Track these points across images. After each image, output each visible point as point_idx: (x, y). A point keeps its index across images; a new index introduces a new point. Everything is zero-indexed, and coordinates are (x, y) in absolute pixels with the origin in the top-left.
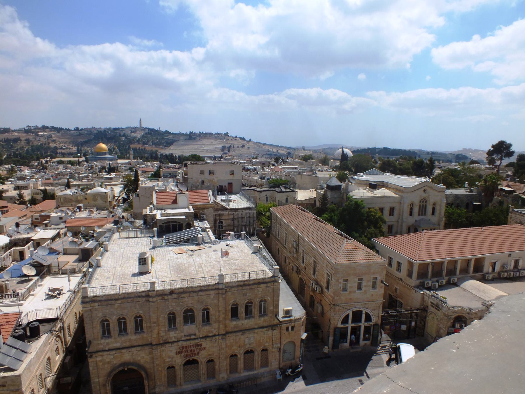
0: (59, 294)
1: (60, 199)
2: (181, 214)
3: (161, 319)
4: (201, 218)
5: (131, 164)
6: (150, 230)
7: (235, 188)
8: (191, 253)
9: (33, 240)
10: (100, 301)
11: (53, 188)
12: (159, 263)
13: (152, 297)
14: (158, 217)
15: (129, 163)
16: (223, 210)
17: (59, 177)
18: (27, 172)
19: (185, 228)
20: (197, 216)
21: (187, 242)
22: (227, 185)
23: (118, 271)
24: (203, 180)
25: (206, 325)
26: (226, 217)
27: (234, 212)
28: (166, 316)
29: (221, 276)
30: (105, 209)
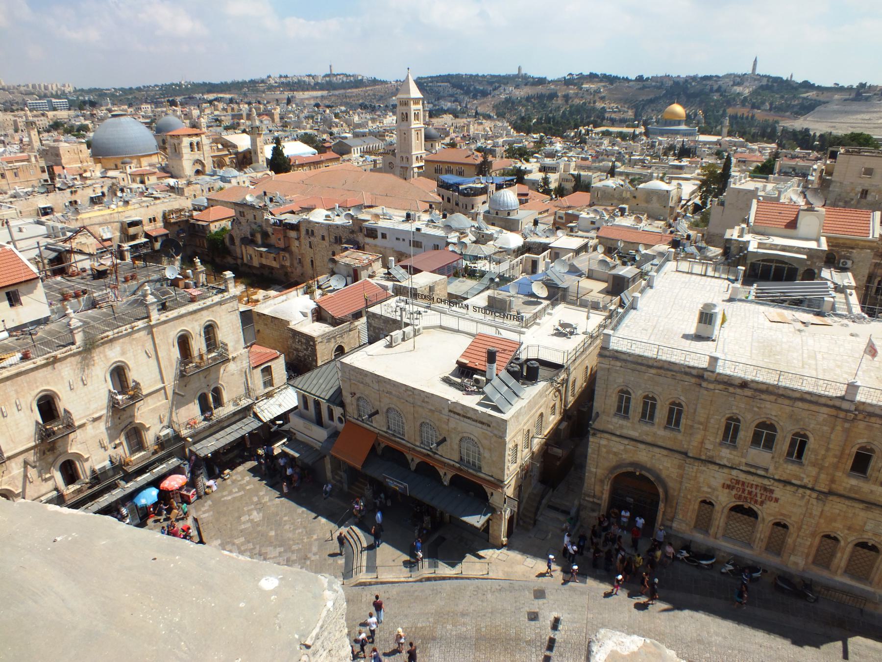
0: (572, 333)
2: (799, 250)
3: (712, 421)
4: (841, 265)
5: (720, 145)
6: (732, 268)
8: (801, 327)
9: (551, 248)
10: (625, 361)
11: (590, 174)
14: (752, 247)
15: (718, 143)
17: (600, 157)
18: (558, 146)
19: (800, 278)
20: (832, 259)
21: (797, 303)
24: (865, 188)
25: (793, 462)
28: (723, 420)
29: (852, 387)
30: (662, 218)
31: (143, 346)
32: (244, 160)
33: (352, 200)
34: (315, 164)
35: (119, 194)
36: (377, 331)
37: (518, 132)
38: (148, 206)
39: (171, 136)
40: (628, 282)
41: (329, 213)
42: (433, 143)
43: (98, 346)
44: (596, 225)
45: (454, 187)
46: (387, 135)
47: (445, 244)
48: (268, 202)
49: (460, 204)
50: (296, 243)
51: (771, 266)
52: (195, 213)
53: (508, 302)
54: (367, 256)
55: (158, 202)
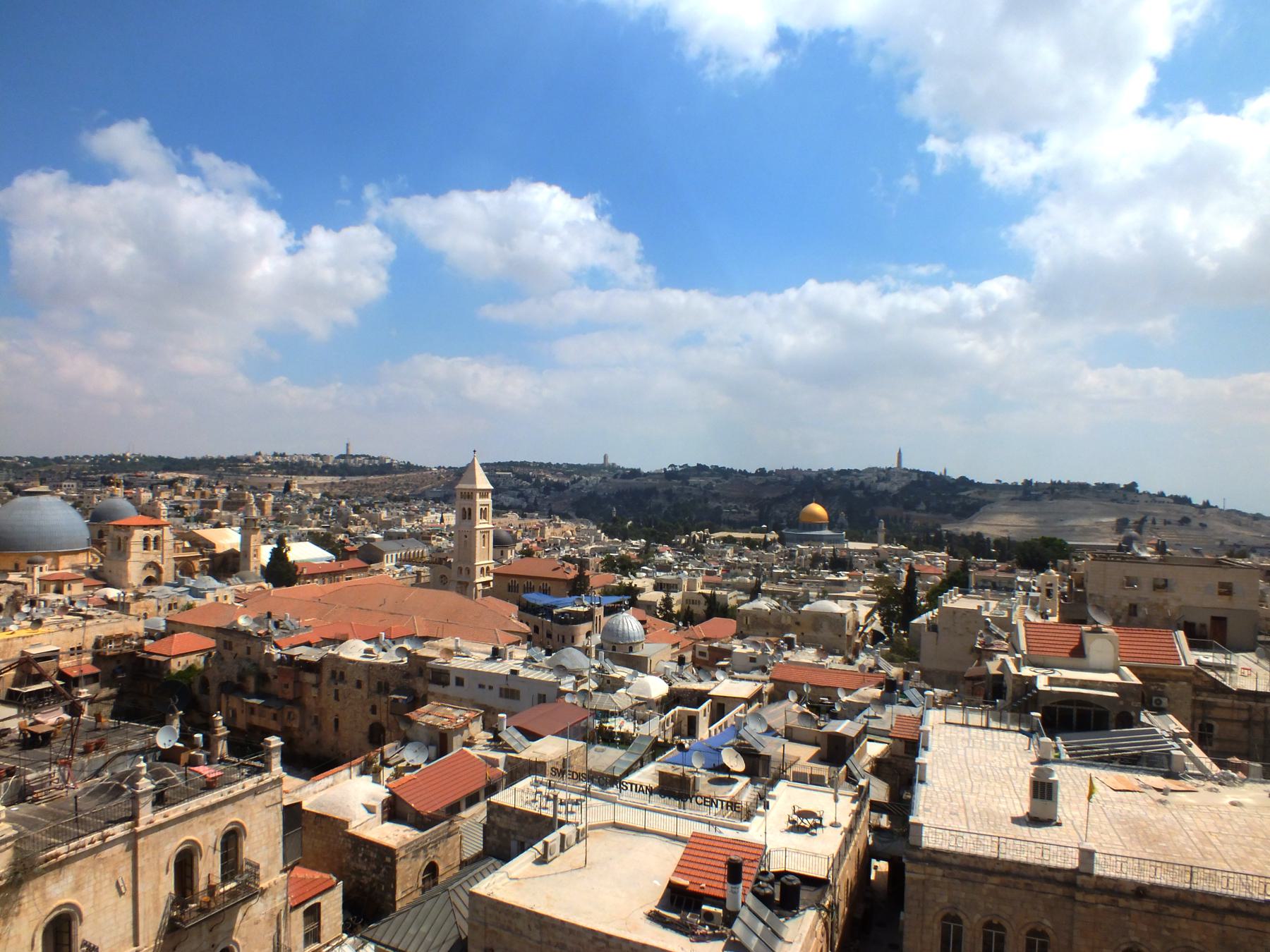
0: (816, 826)
1: (745, 618)
4: (1154, 705)
5: (878, 554)
7: (1233, 630)
8: (1159, 796)
9: (712, 697)
10: (950, 866)
11: (724, 593)
12: (1074, 805)
13: (1082, 889)
15: (873, 551)
16: (1213, 691)
17: (732, 571)
18: (668, 556)
19: (1113, 725)
21: (1131, 762)
22: (1208, 622)
23: (973, 803)
24: (1133, 602)
26: (1225, 714)
27: (1253, 704)
31: (115, 872)
32: (225, 566)
33: (398, 628)
34: (330, 575)
35: (25, 609)
36: (504, 835)
38: (72, 629)
39: (115, 526)
40: (853, 742)
41: (371, 646)
42: (504, 550)
43: (36, 876)
44: (759, 663)
45: (547, 611)
46: (434, 538)
48: (273, 629)
49: (555, 635)
50: (314, 692)
51: (1072, 710)
52: (147, 642)
53: (692, 780)
55: (89, 622)
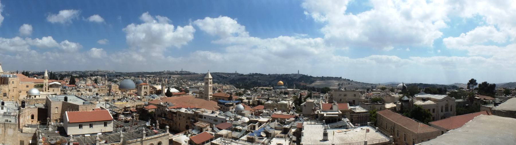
8: (345, 132)
11: (261, 100)
14: (325, 115)
15: (293, 91)
17: (263, 95)
18: (249, 92)
20: (343, 115)
21: (340, 127)
32: (159, 93)
33: (192, 106)
37: (237, 88)
41: (186, 110)
45: (224, 104)
47: (225, 121)
48: (167, 105)
49: (225, 109)
50: (175, 118)
52: (145, 106)
54: (205, 124)
